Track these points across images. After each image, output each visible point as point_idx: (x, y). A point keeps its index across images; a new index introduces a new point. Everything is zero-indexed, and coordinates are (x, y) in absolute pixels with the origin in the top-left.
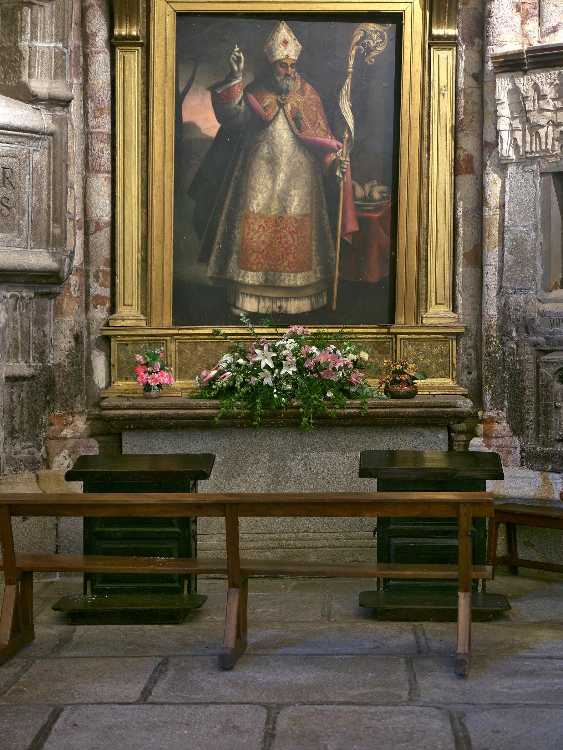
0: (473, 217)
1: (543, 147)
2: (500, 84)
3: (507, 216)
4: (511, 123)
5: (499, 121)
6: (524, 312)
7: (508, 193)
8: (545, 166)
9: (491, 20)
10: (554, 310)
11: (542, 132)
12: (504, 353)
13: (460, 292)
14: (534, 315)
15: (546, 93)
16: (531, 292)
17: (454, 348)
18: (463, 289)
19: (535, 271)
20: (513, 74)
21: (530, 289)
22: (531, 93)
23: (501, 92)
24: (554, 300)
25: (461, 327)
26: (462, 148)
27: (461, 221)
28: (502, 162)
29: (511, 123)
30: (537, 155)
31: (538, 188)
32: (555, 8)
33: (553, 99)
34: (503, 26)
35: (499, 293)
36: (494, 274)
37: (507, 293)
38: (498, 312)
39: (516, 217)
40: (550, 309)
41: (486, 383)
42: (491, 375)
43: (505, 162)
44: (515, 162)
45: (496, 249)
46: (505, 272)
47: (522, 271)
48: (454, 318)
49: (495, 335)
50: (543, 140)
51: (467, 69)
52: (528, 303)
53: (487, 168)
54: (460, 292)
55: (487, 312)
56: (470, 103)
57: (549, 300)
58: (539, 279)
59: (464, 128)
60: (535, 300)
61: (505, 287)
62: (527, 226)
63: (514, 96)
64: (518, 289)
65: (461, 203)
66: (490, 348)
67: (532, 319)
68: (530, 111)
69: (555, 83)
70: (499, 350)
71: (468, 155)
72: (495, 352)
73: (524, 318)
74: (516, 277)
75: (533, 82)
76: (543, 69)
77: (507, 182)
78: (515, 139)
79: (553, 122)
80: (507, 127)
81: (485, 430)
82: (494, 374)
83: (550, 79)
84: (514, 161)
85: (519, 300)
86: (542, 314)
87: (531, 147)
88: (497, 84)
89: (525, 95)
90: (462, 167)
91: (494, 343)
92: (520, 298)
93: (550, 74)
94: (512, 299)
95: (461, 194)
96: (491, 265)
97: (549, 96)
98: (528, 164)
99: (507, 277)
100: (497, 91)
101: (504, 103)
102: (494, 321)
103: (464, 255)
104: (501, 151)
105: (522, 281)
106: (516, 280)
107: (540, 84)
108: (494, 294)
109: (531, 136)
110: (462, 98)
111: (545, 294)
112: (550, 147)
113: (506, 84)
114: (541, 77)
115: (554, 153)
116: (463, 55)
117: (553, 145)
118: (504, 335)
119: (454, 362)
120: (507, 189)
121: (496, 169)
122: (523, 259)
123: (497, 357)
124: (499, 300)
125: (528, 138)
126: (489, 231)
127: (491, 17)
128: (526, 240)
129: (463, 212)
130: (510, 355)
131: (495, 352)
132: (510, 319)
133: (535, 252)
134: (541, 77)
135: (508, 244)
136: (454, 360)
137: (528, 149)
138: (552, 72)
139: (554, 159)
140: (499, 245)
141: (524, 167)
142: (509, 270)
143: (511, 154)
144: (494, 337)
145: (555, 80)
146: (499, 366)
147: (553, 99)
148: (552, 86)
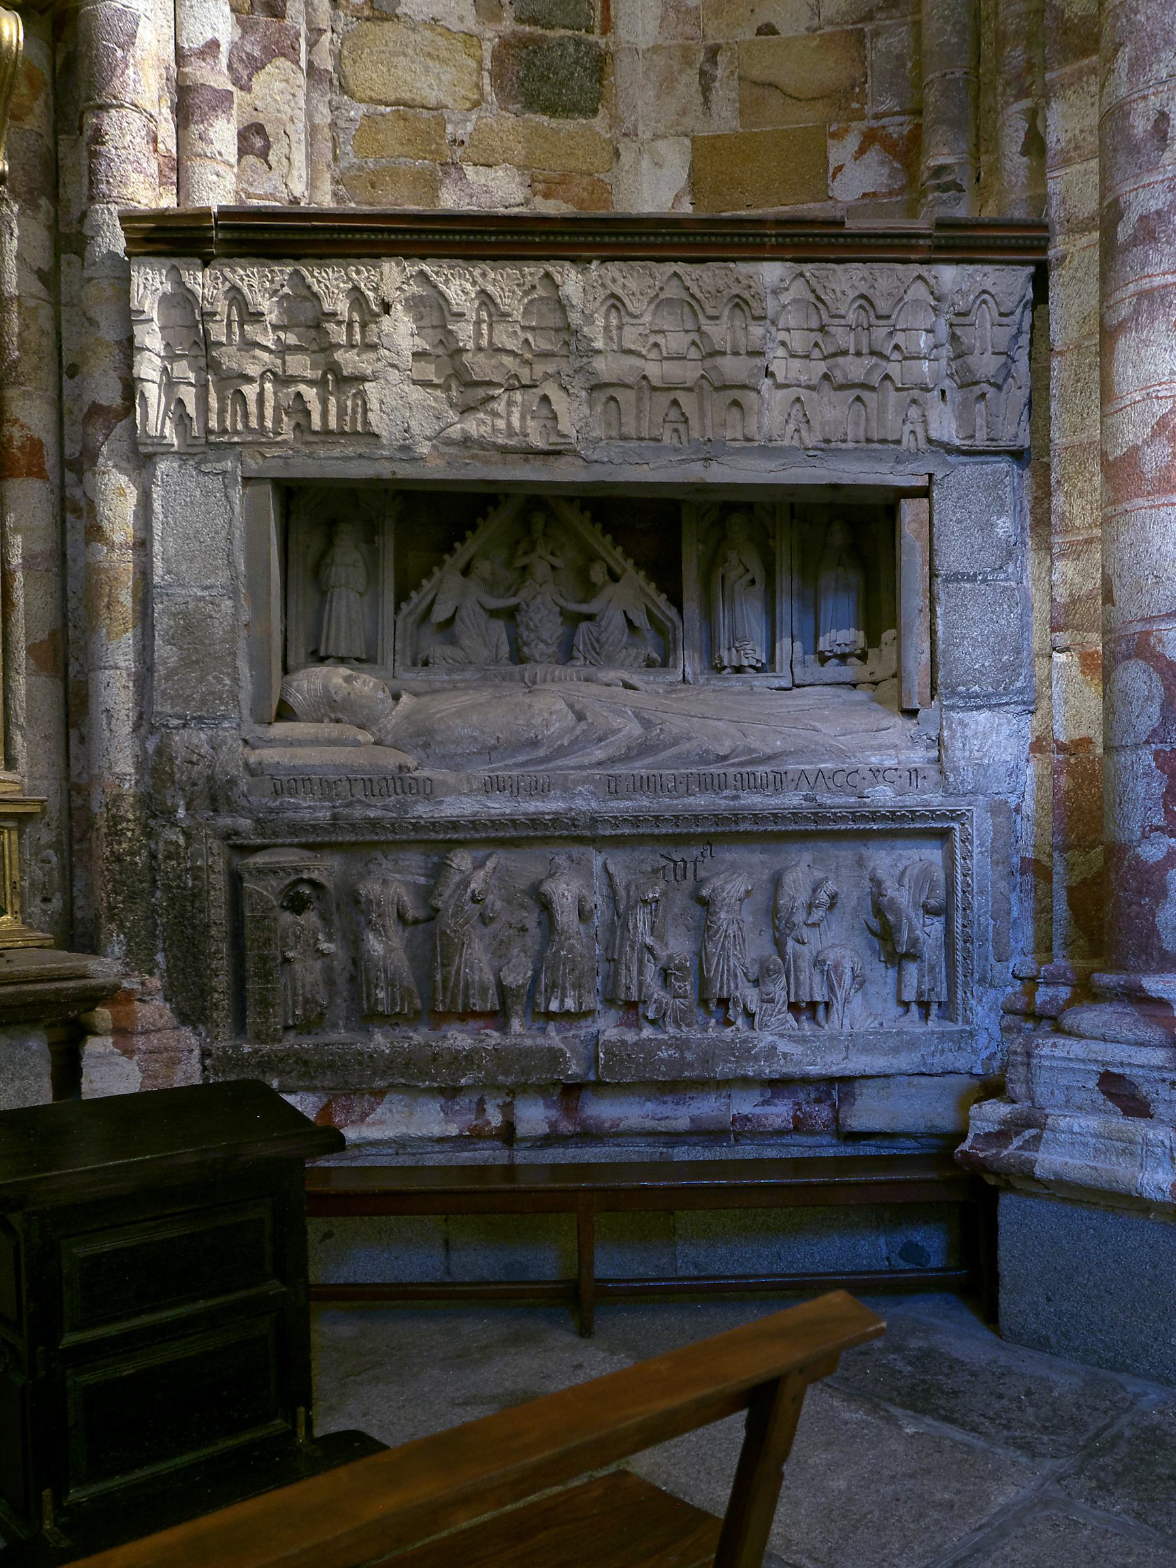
0: (47, 570)
1: (254, 423)
2: (142, 281)
3: (158, 565)
4: (165, 368)
5: (138, 358)
6: (209, 766)
7: (161, 517)
8: (254, 465)
9: (103, 148)
10: (285, 761)
11: (250, 391)
12: (153, 856)
13: (20, 727)
14: (234, 772)
15: (260, 308)
16: (226, 724)
17: (15, 847)
18: (29, 722)
19: (236, 681)
20: (175, 261)
21: (224, 717)
22: (222, 306)
23: (144, 297)
24: (281, 740)
25: (33, 801)
26: (16, 421)
27: (19, 575)
28: (142, 449)
29: (165, 368)
30: (236, 439)
31: (237, 509)
32: (215, 178)
33: (275, 328)
34: (130, 168)
35: (136, 727)
36: (125, 687)
37: (167, 726)
38: (136, 768)
39: (184, 568)
40: (276, 759)
41: (111, 919)
42: (123, 902)
43: (150, 449)
44: (176, 453)
45: (129, 635)
46: (159, 681)
47: (201, 680)
48: (12, 782)
49: (131, 816)
50: (252, 408)
51: (25, 255)
52: (220, 746)
53: (101, 460)
54: (20, 727)
55: (110, 768)
56: (33, 328)
57: (270, 741)
58: (245, 697)
59: (22, 379)
60: (235, 740)
61: (160, 713)
62: (211, 587)
63: (173, 311)
64: (194, 718)
65: (19, 539)
66: (120, 843)
67: (229, 781)
68: (221, 344)
69: (281, 293)
70: (141, 848)
71: (31, 439)
72: (132, 854)
73: (210, 778)
74: (188, 692)
75: (228, 285)
76: (254, 260)
77: (157, 493)
78: (180, 402)
79: (274, 374)
80: (155, 376)
81: (115, 1020)
82: (132, 897)
83: (272, 282)
84: (175, 449)
85: (196, 741)
87: (221, 420)
88: (135, 280)
89: (208, 308)
90: (18, 461)
91: (129, 834)
92: (198, 736)
93: (271, 272)
94: (177, 738)
95: (18, 520)
96: (117, 668)
97: (268, 318)
98: (211, 458)
99: (164, 693)
100: (134, 293)
101: (152, 320)
102: (127, 786)
103: (28, 649)
104: (144, 425)
105: (204, 702)
106: (187, 700)
107: (246, 290)
108: (127, 729)
109: (221, 400)
110: (14, 316)
111: (260, 730)
112: (269, 424)
113: (158, 280)
114: (248, 276)
115: (279, 439)
116: (14, 225)
117: (277, 421)
118: (154, 816)
119: (16, 878)
120: (157, 506)
121: (124, 464)
122: (205, 656)
123: (136, 863)
124: (138, 742)
125: (214, 402)
126: (109, 596)
127: (103, 143)
128: (211, 617)
129: (23, 558)
130: (168, 857)
131: (132, 854)
132: (173, 782)
133: (234, 641)
134: (248, 276)
135: (163, 623)
136: (16, 872)
137: (213, 424)
138: (276, 268)
139: (276, 451)
140: (134, 627)
141: (199, 464)
142: (168, 678)
143: (167, 432)
144: (129, 820)
145: (282, 286)
146: (141, 882)
147: (275, 328)
148: (275, 299)
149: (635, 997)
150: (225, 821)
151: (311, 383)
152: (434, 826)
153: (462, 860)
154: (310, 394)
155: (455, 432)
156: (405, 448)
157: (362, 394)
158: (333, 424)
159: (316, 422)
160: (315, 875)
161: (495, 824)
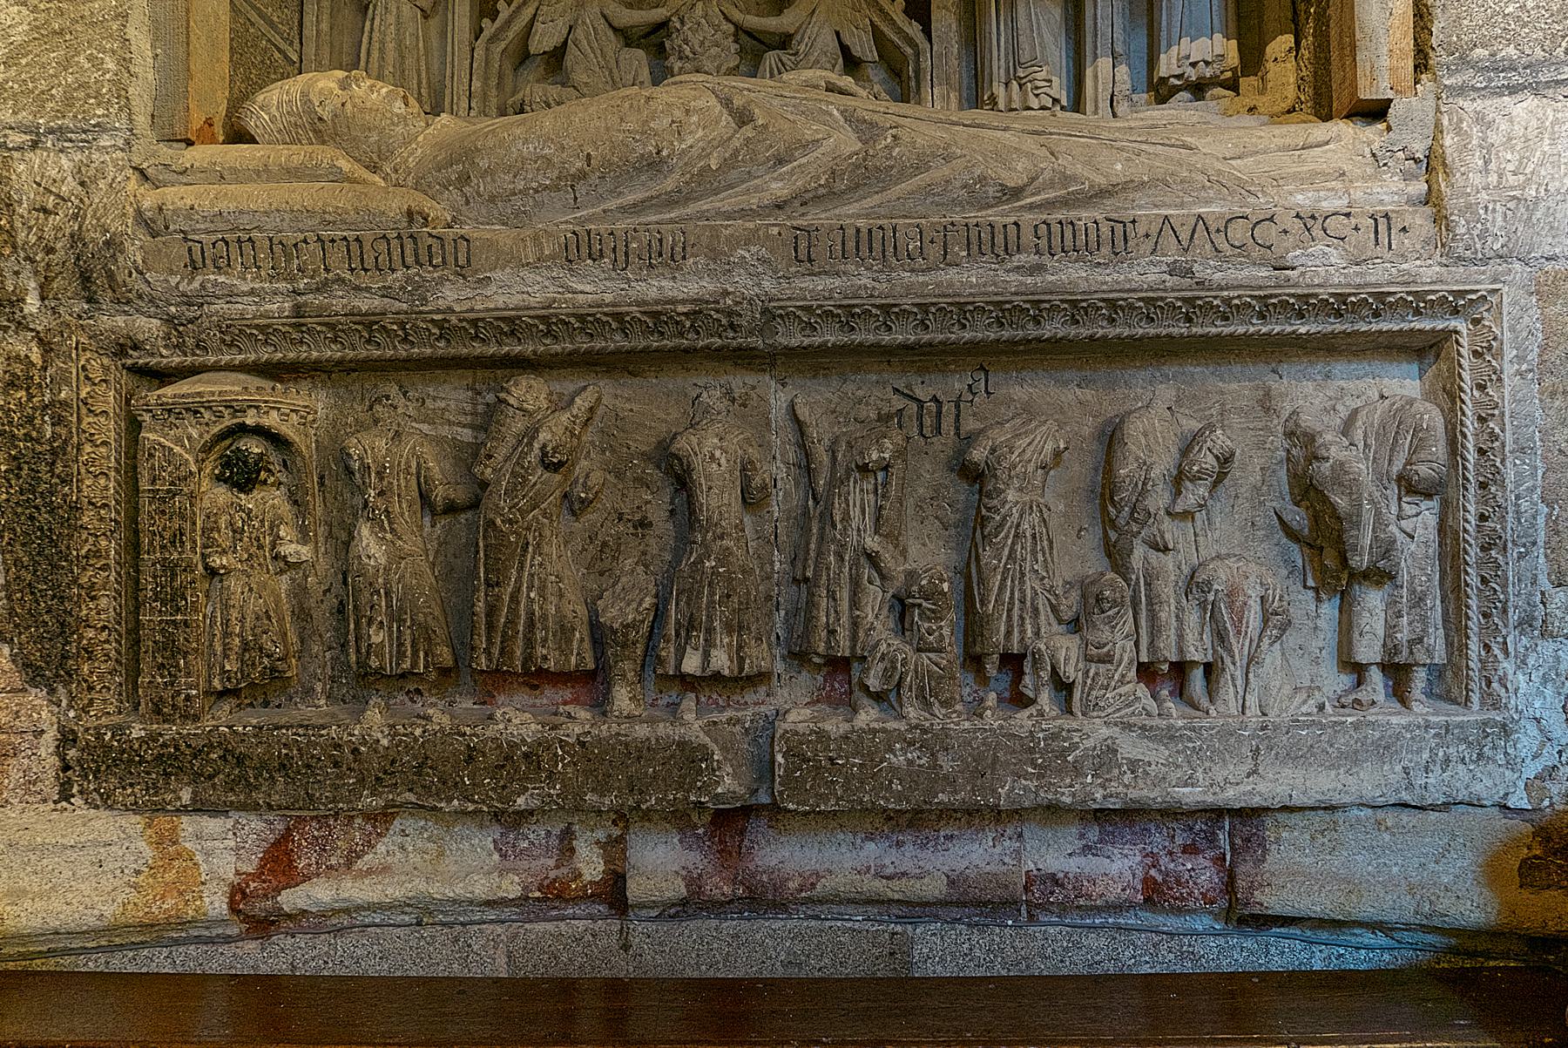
6: (75, 217)
14: (117, 226)
16: (105, 141)
19: (125, 62)
47: (65, 64)
52: (94, 180)
58: (141, 94)
64: (51, 131)
67: (107, 243)
73: (76, 239)
86: (151, 225)
105: (69, 101)
106: (42, 99)
111: (166, 152)
149: (844, 649)
152: (475, 326)
153: (529, 392)
161: (586, 321)
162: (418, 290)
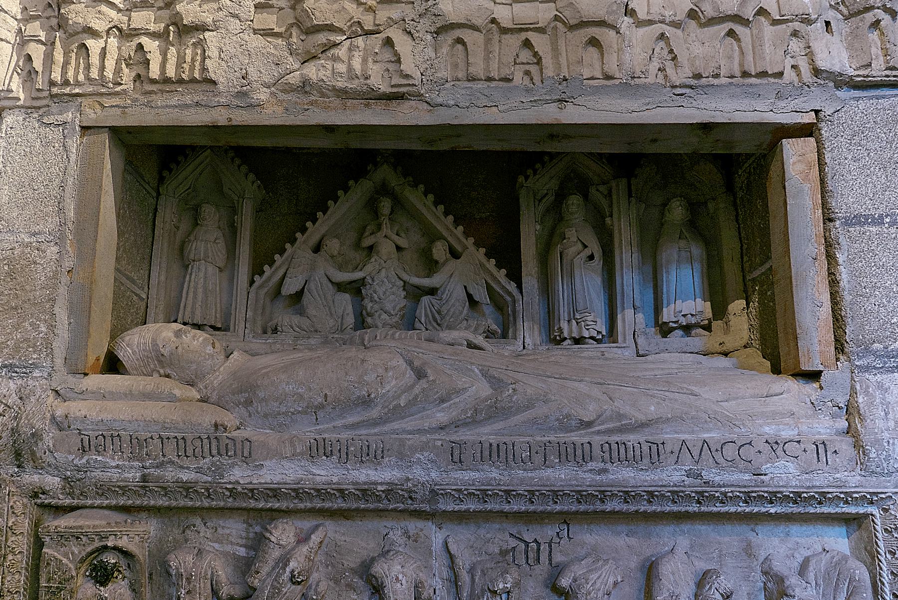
50: (95, 60)
86: (61, 424)
112: (109, 74)
137: (57, 76)
150: (32, 478)
151: (154, 35)
154: (151, 46)
155: (294, 79)
156: (242, 94)
157: (201, 43)
158: (171, 72)
159: (155, 71)
160: (123, 543)
162: (219, 470)
